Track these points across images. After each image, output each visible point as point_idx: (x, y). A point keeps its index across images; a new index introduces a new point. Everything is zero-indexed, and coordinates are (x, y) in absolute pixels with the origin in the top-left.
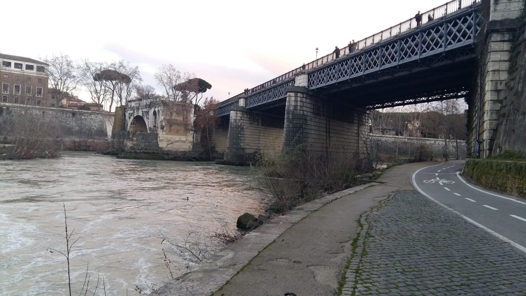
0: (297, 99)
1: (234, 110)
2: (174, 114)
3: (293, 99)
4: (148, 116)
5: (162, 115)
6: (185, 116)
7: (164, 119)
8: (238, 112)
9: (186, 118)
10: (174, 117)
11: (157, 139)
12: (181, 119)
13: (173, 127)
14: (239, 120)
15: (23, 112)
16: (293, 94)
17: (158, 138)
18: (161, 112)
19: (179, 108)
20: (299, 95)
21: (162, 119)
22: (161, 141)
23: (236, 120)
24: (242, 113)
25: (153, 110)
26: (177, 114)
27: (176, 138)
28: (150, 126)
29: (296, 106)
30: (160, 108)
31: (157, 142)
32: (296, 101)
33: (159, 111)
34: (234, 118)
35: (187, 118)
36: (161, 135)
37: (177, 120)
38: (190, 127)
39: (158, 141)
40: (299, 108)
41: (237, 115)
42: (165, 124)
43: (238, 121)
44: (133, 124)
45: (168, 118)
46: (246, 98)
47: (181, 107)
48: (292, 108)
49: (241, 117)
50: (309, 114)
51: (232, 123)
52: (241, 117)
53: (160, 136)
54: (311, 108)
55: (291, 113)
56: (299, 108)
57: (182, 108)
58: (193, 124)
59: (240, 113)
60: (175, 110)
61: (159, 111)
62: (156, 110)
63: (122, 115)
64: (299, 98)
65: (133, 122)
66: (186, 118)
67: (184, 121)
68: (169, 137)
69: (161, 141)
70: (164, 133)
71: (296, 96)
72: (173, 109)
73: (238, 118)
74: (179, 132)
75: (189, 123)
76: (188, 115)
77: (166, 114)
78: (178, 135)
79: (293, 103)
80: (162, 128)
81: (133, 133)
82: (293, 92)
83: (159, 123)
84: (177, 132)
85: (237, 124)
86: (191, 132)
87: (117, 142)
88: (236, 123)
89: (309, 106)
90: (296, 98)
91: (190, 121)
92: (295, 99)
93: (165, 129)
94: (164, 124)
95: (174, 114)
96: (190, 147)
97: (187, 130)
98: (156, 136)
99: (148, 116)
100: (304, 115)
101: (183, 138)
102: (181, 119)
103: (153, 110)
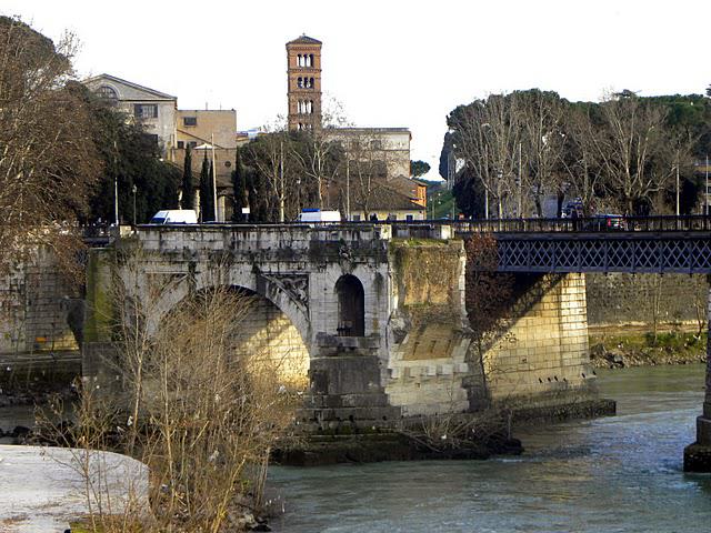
4: (301, 292)
11: (379, 381)
18: (390, 283)
25: (334, 273)
31: (381, 391)
33: (379, 279)
39: (383, 384)
61: (379, 279)
62: (364, 274)
70: (402, 353)
78: (432, 358)
80: (399, 336)
84: (432, 351)
93: (405, 342)
96: (461, 398)
99: (301, 292)
103: (334, 273)
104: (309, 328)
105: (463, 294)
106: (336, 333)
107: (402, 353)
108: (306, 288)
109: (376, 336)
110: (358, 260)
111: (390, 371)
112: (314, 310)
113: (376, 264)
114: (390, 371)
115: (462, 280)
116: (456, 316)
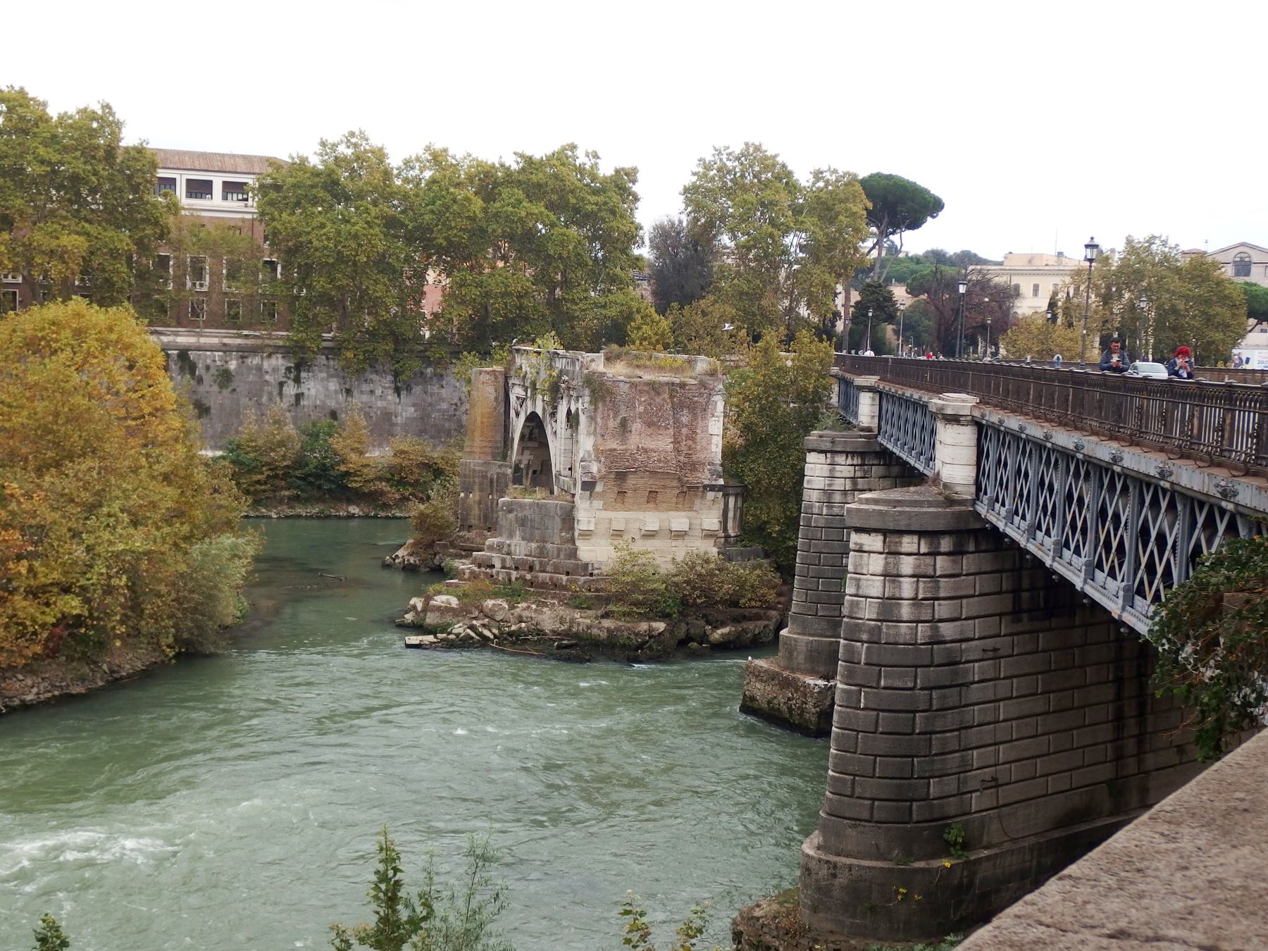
0: (897, 565)
2: (637, 426)
3: (876, 563)
6: (684, 431)
8: (840, 459)
9: (688, 438)
10: (638, 438)
11: (572, 529)
12: (662, 443)
13: (631, 481)
14: (845, 492)
15: (233, 365)
16: (874, 542)
19: (658, 400)
20: (908, 544)
22: (587, 534)
23: (828, 493)
24: (857, 461)
26: (650, 424)
27: (652, 519)
29: (888, 604)
32: (891, 576)
34: (820, 483)
35: (692, 437)
36: (588, 514)
37: (646, 451)
38: (705, 478)
40: (906, 611)
43: (837, 498)
44: (530, 439)
45: (613, 444)
46: (881, 394)
47: (666, 396)
48: (868, 612)
49: (853, 479)
50: (975, 628)
52: (853, 479)
54: (1000, 593)
55: (865, 637)
56: (906, 611)
57: (672, 397)
59: (849, 461)
60: (641, 409)
63: (496, 399)
64: (911, 559)
65: (527, 432)
66: (687, 438)
67: (678, 451)
68: (620, 518)
69: (587, 534)
70: (598, 504)
72: (630, 405)
73: (839, 484)
74: (660, 497)
75: (702, 456)
76: (700, 424)
77: (606, 426)
78: (656, 509)
79: (874, 587)
80: (588, 486)
81: (535, 472)
82: (876, 531)
85: (836, 511)
86: (711, 495)
87: (480, 503)
89: (980, 584)
90: (891, 559)
92: (887, 564)
93: (599, 488)
94: (594, 468)
100: (936, 640)
101: (679, 521)
102: (662, 443)
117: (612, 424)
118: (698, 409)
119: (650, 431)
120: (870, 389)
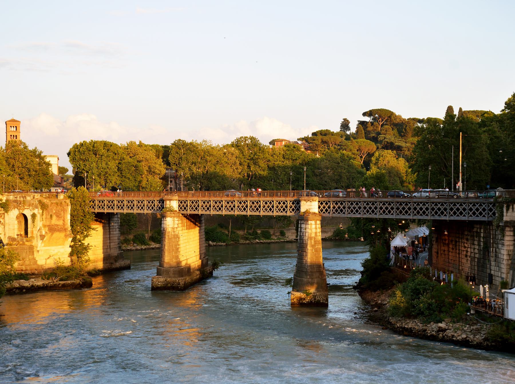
1: (171, 217)
2: (54, 217)
3: (314, 226)
5: (41, 221)
7: (45, 226)
8: (176, 219)
10: (55, 221)
11: (33, 254)
14: (177, 228)
17: (35, 253)
21: (41, 226)
23: (173, 228)
26: (57, 216)
28: (7, 236)
30: (36, 211)
32: (316, 228)
33: (34, 216)
34: (171, 226)
37: (57, 225)
39: (35, 256)
41: (174, 222)
42: (46, 233)
45: (48, 223)
49: (178, 224)
51: (169, 232)
53: (38, 249)
58: (70, 228)
60: (54, 212)
61: (34, 216)
62: (28, 213)
70: (43, 244)
71: (316, 224)
73: (176, 226)
77: (46, 218)
79: (314, 231)
80: (42, 237)
83: (35, 232)
88: (174, 232)
91: (67, 224)
93: (45, 239)
94: (44, 233)
95: (54, 217)
97: (66, 236)
98: (31, 249)
102: (61, 223)
104: (5, 234)
105: (69, 221)
106: (16, 237)
107: (43, 244)
108: (4, 218)
109: (32, 237)
110: (26, 207)
111: (38, 251)
112: (6, 227)
113: (33, 209)
114: (38, 251)
115: (69, 217)
116: (65, 230)
117: (49, 217)
118: (64, 211)
119: (58, 218)
120: (176, 200)
